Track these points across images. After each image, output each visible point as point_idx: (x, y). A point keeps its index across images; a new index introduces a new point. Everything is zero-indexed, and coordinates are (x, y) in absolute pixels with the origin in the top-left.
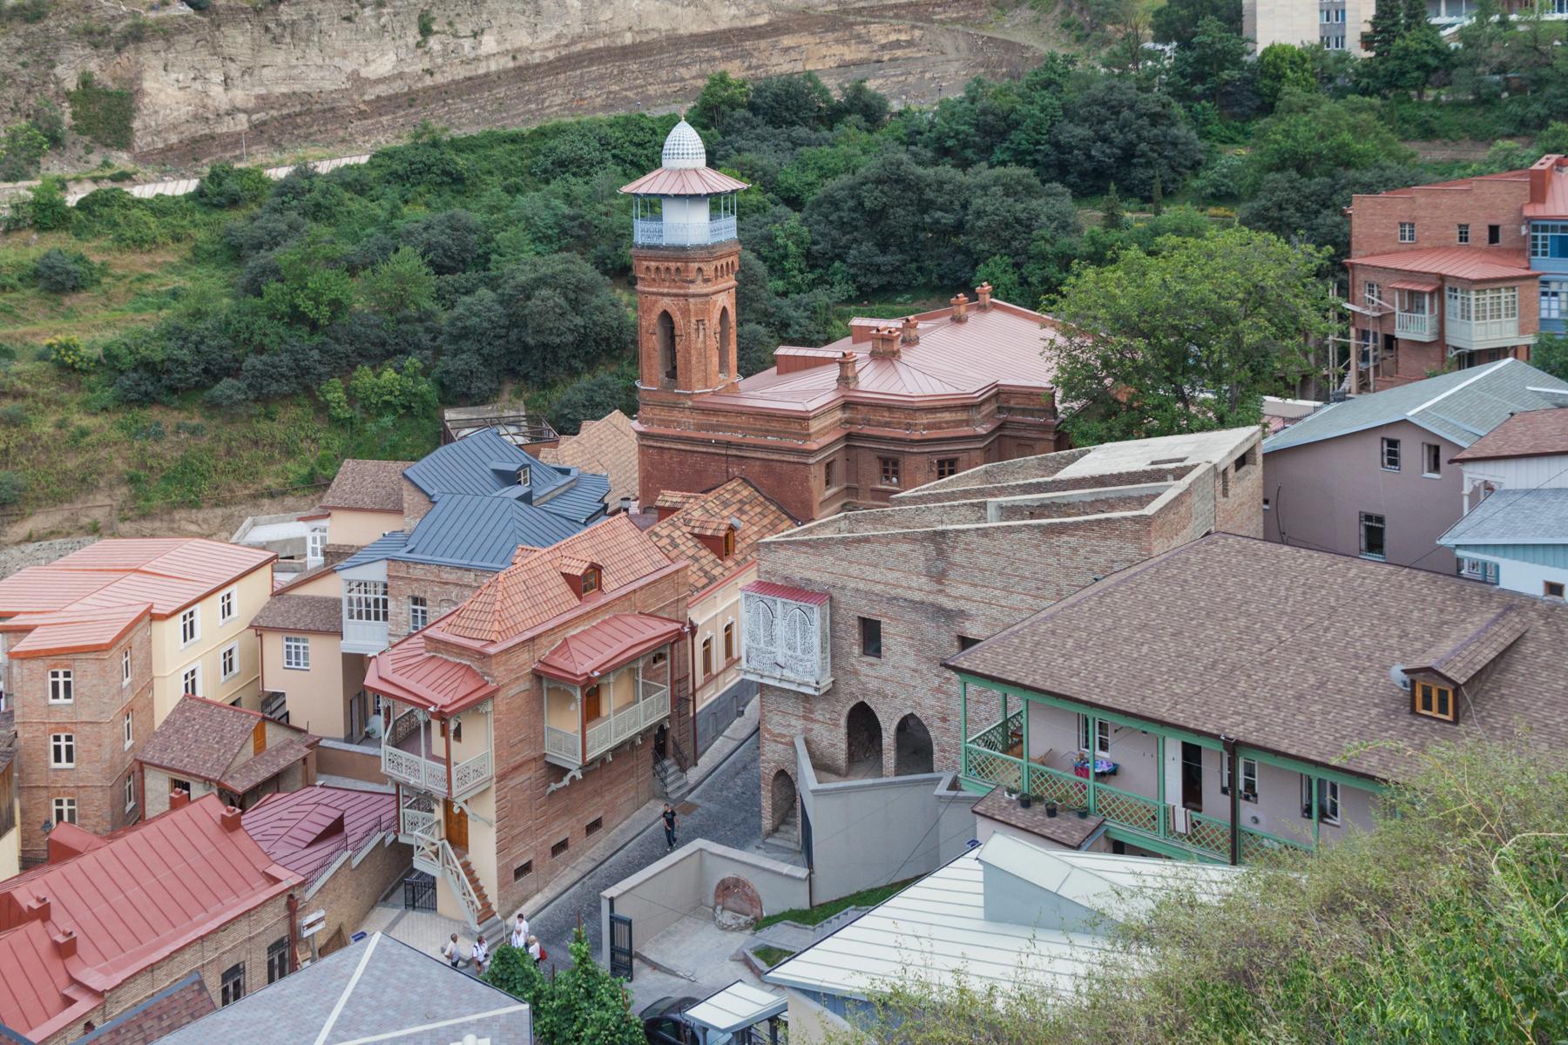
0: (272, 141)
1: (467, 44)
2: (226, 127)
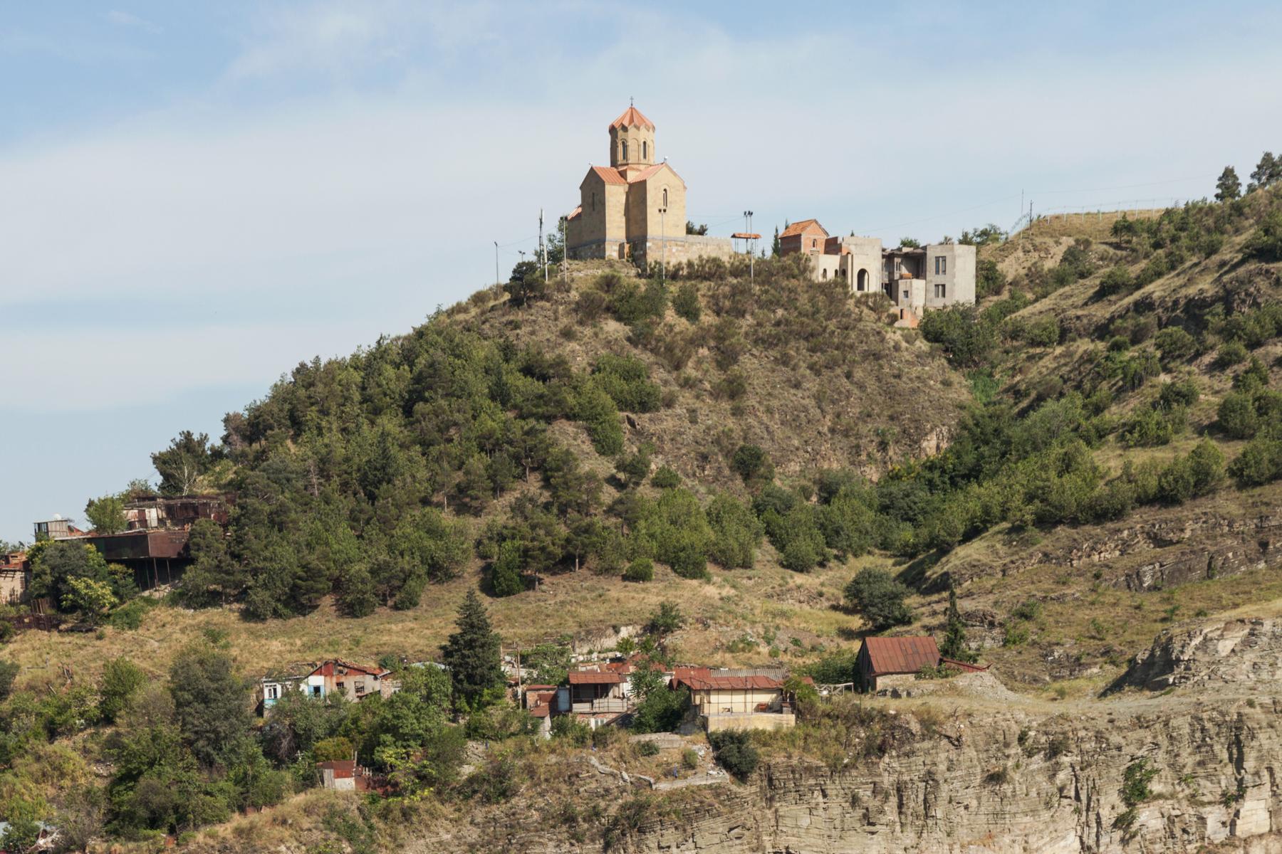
1: (1215, 816)
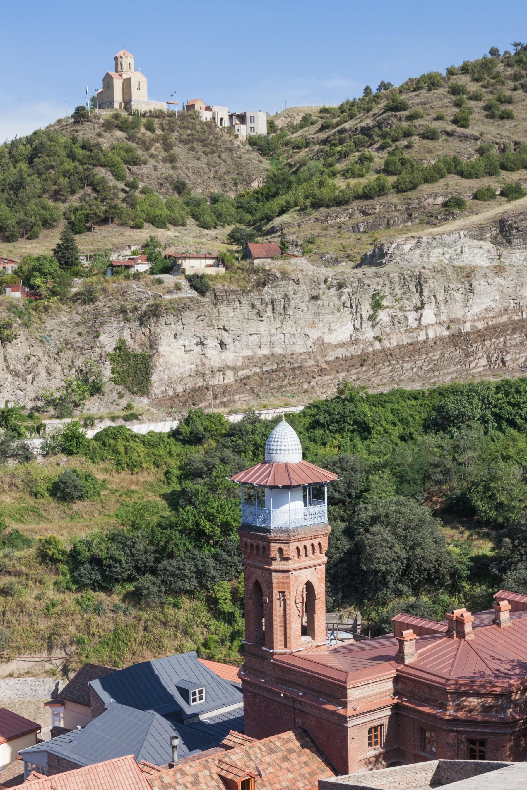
0: (252, 390)
1: (412, 316)
2: (217, 380)
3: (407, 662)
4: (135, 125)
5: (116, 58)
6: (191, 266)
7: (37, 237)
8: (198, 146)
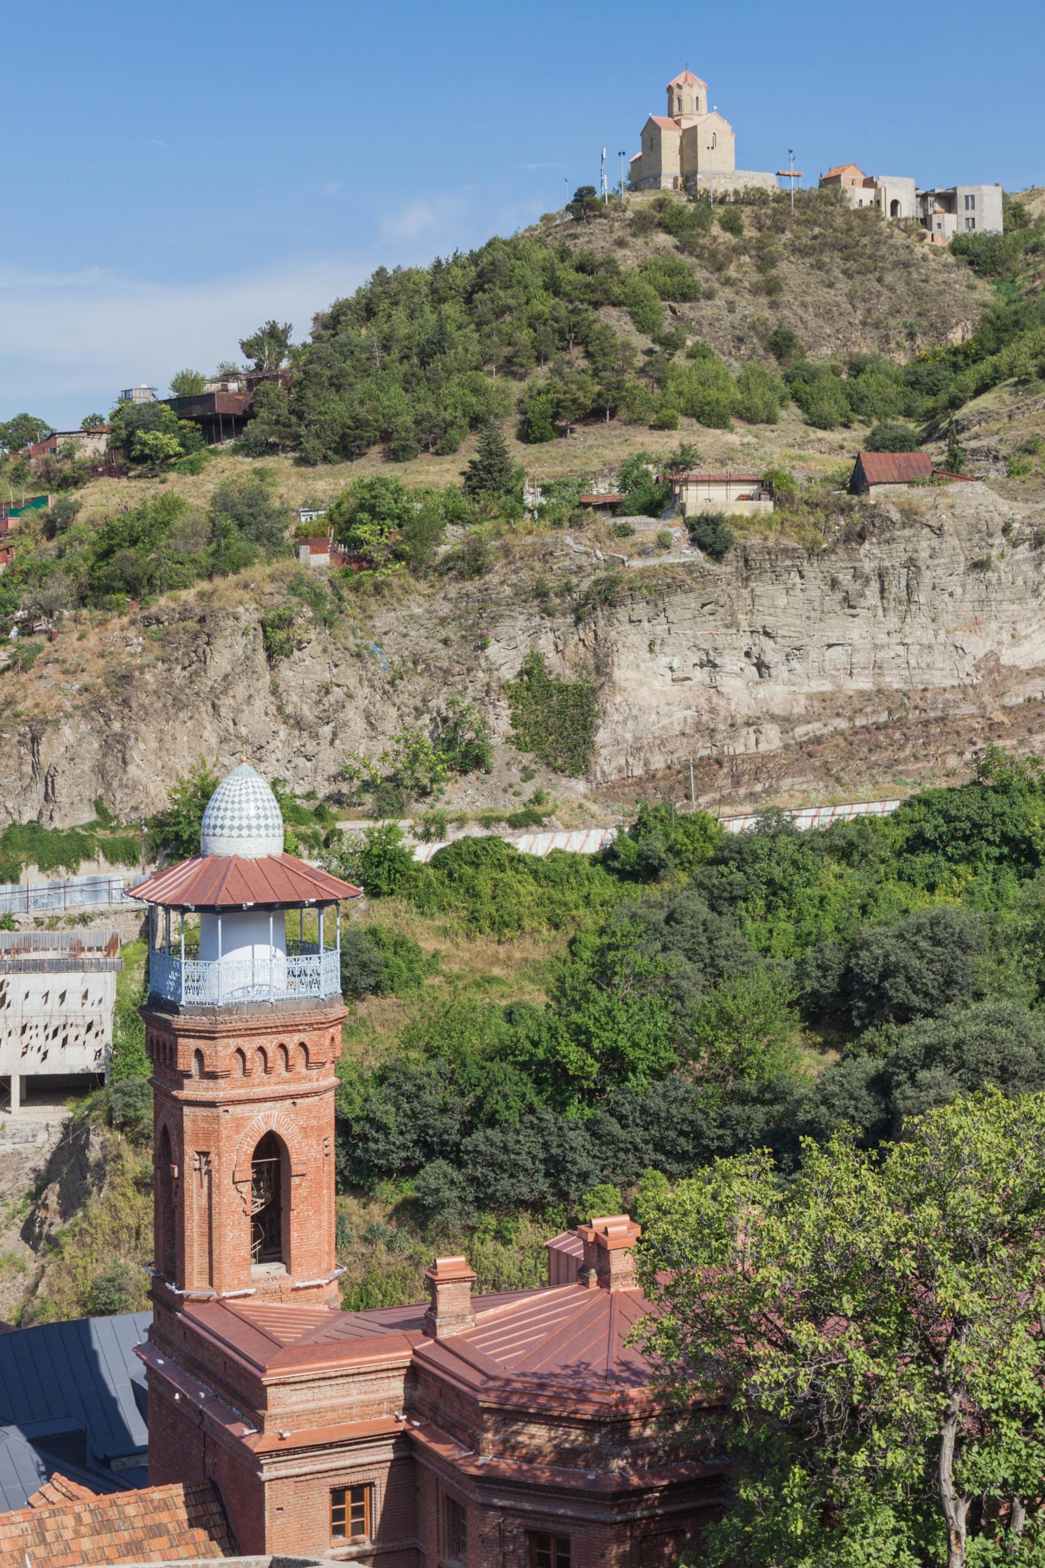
2: (743, 745)
3: (443, 1334)
4: (701, 220)
5: (670, 89)
6: (697, 499)
7: (455, 451)
8: (834, 260)
